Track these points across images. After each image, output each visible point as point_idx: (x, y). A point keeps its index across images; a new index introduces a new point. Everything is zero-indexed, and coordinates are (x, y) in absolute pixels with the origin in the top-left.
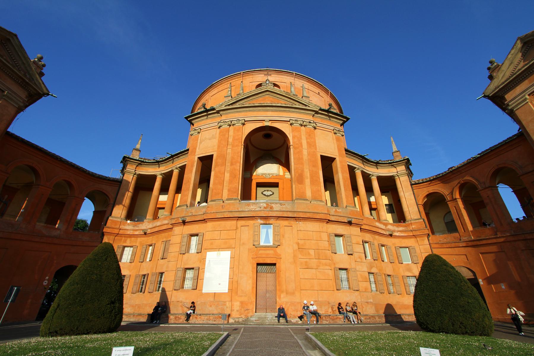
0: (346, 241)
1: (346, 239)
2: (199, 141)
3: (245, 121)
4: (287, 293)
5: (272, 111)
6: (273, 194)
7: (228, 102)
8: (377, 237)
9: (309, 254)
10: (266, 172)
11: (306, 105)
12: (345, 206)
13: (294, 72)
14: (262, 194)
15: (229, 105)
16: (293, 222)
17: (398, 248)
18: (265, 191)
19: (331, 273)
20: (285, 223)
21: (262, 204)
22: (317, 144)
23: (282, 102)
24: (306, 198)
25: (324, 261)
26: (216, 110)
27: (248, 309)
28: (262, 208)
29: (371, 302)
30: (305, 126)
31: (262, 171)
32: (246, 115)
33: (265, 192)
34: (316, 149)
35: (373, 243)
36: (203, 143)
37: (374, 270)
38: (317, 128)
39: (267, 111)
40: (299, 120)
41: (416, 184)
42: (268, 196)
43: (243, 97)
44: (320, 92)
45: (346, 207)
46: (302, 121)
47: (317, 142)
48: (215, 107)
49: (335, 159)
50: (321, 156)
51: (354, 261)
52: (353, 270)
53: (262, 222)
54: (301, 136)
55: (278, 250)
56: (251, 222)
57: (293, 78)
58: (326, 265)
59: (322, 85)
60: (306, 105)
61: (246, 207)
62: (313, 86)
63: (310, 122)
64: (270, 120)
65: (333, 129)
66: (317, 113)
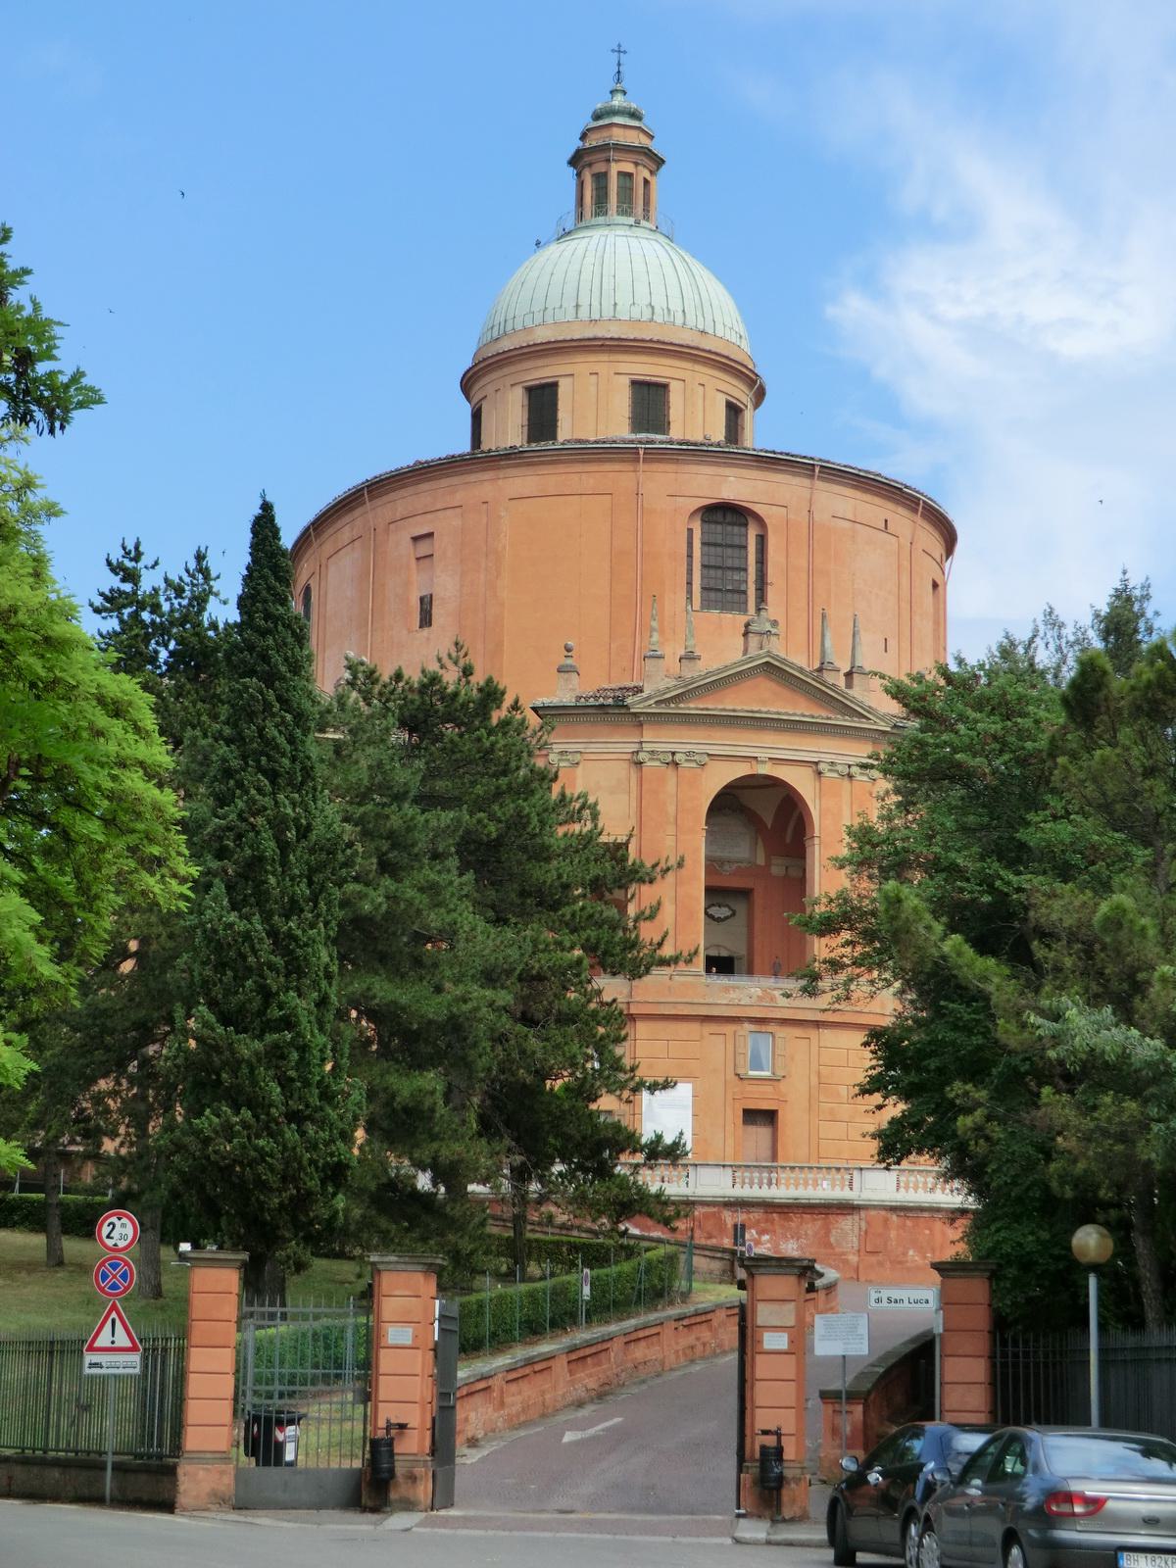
5: (776, 730)
6: (734, 914)
18: (713, 905)
20: (797, 1032)
21: (753, 990)
23: (801, 709)
28: (753, 1001)
30: (850, 776)
39: (763, 729)
40: (838, 760)
42: (719, 920)
44: (889, 516)
53: (752, 1027)
55: (783, 1086)
56: (729, 1029)
57: (806, 482)
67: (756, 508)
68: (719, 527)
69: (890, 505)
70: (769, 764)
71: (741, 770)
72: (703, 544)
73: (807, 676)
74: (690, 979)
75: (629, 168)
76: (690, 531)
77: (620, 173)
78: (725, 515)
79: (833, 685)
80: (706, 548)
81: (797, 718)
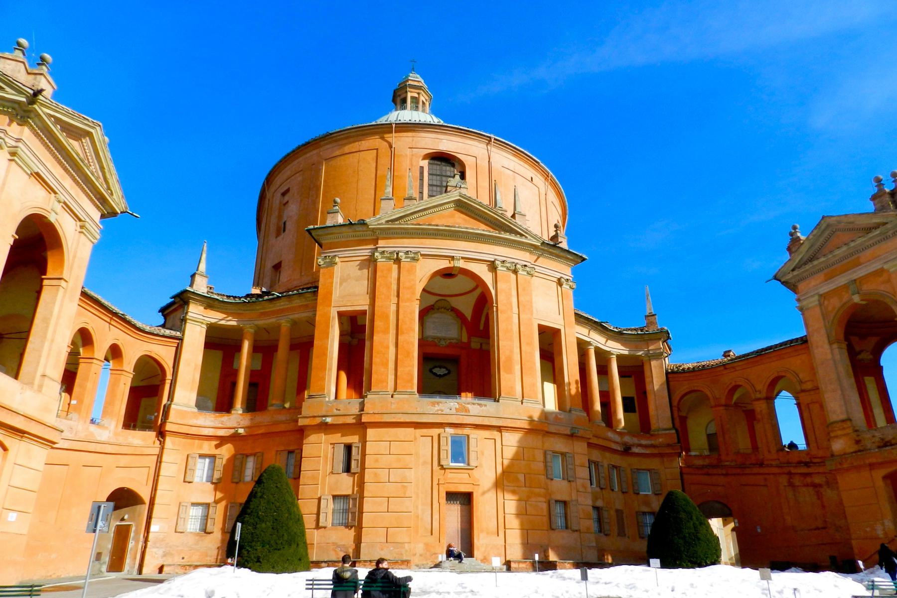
0: (568, 463)
1: (567, 459)
2: (336, 279)
3: (422, 255)
4: (488, 533)
6: (449, 373)
7: (391, 216)
8: (607, 454)
9: (517, 480)
10: (440, 335)
11: (522, 235)
12: (568, 411)
13: (492, 136)
14: (431, 371)
15: (393, 221)
16: (496, 434)
17: (635, 470)
18: (435, 367)
19: (545, 506)
22: (534, 305)
23: (482, 229)
24: (516, 396)
25: (537, 490)
26: (370, 227)
27: (436, 552)
28: (453, 411)
29: (593, 546)
30: (515, 272)
31: (433, 333)
33: (436, 369)
34: (532, 314)
35: (602, 464)
36: (344, 284)
37: (599, 503)
38: (536, 274)
41: (673, 372)
42: (440, 376)
43: (416, 207)
45: (570, 411)
46: (513, 263)
47: (534, 300)
48: (368, 221)
49: (558, 331)
50: (540, 327)
51: (575, 491)
52: (574, 503)
54: (510, 289)
56: (435, 432)
58: (539, 495)
60: (522, 235)
61: (429, 407)
62: (522, 163)
63: (525, 266)
64: (463, 258)
65: (559, 277)
66: (535, 247)
68: (438, 167)
69: (534, 171)
70: (462, 261)
71: (444, 264)
72: (429, 174)
73: (485, 208)
74: (406, 396)
75: (416, 95)
76: (422, 168)
77: (412, 98)
78: (442, 159)
79: (502, 214)
80: (431, 176)
81: (479, 232)
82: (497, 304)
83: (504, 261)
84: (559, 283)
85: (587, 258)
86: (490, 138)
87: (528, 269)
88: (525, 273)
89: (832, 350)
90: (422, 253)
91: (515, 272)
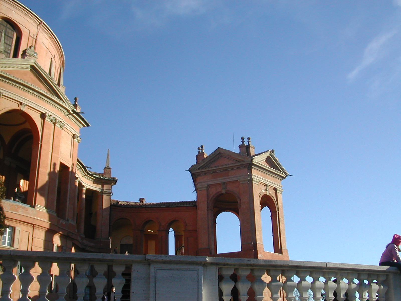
12: (66, 219)
23: (43, 89)
30: (55, 124)
32: (4, 87)
43: (7, 61)
59: (60, 47)
63: (61, 122)
64: (27, 105)
65: (74, 134)
66: (68, 111)
67: (20, 26)
71: (15, 106)
82: (41, 142)
83: (50, 115)
84: (74, 137)
85: (90, 126)
86: (41, 21)
87: (61, 124)
88: (59, 126)
89: (208, 213)
90: (3, 94)
91: (55, 124)
